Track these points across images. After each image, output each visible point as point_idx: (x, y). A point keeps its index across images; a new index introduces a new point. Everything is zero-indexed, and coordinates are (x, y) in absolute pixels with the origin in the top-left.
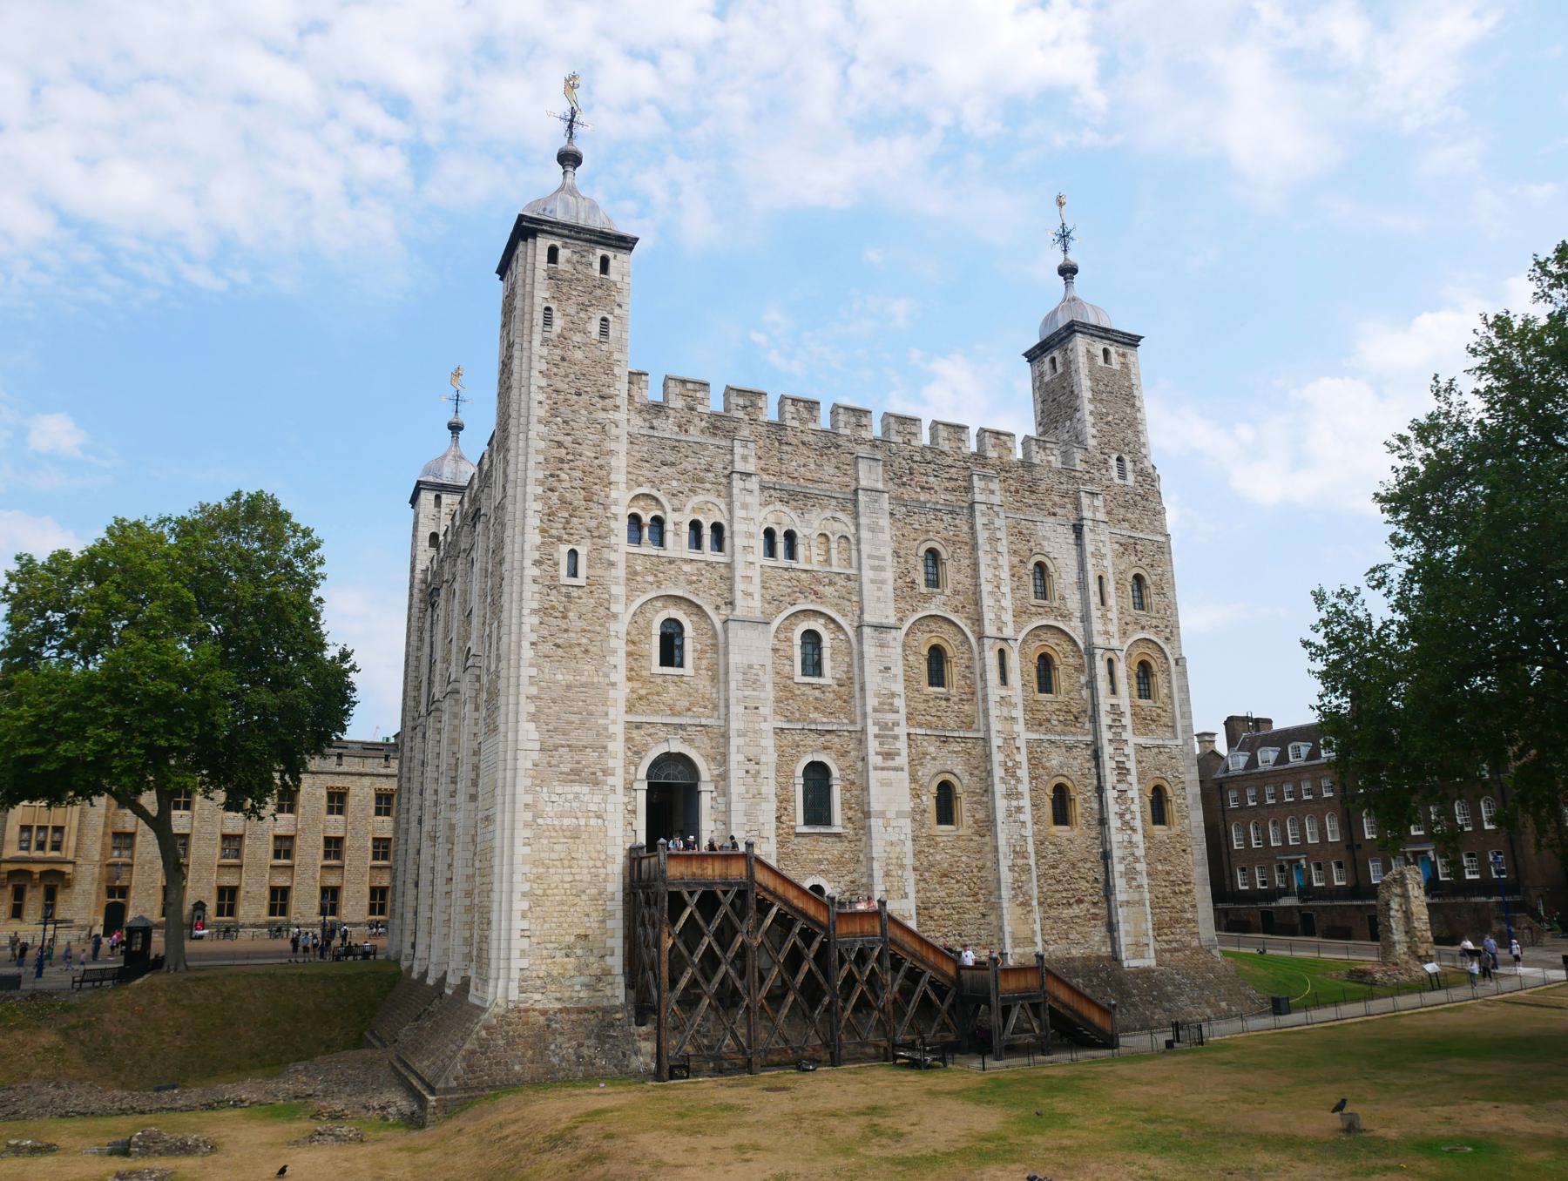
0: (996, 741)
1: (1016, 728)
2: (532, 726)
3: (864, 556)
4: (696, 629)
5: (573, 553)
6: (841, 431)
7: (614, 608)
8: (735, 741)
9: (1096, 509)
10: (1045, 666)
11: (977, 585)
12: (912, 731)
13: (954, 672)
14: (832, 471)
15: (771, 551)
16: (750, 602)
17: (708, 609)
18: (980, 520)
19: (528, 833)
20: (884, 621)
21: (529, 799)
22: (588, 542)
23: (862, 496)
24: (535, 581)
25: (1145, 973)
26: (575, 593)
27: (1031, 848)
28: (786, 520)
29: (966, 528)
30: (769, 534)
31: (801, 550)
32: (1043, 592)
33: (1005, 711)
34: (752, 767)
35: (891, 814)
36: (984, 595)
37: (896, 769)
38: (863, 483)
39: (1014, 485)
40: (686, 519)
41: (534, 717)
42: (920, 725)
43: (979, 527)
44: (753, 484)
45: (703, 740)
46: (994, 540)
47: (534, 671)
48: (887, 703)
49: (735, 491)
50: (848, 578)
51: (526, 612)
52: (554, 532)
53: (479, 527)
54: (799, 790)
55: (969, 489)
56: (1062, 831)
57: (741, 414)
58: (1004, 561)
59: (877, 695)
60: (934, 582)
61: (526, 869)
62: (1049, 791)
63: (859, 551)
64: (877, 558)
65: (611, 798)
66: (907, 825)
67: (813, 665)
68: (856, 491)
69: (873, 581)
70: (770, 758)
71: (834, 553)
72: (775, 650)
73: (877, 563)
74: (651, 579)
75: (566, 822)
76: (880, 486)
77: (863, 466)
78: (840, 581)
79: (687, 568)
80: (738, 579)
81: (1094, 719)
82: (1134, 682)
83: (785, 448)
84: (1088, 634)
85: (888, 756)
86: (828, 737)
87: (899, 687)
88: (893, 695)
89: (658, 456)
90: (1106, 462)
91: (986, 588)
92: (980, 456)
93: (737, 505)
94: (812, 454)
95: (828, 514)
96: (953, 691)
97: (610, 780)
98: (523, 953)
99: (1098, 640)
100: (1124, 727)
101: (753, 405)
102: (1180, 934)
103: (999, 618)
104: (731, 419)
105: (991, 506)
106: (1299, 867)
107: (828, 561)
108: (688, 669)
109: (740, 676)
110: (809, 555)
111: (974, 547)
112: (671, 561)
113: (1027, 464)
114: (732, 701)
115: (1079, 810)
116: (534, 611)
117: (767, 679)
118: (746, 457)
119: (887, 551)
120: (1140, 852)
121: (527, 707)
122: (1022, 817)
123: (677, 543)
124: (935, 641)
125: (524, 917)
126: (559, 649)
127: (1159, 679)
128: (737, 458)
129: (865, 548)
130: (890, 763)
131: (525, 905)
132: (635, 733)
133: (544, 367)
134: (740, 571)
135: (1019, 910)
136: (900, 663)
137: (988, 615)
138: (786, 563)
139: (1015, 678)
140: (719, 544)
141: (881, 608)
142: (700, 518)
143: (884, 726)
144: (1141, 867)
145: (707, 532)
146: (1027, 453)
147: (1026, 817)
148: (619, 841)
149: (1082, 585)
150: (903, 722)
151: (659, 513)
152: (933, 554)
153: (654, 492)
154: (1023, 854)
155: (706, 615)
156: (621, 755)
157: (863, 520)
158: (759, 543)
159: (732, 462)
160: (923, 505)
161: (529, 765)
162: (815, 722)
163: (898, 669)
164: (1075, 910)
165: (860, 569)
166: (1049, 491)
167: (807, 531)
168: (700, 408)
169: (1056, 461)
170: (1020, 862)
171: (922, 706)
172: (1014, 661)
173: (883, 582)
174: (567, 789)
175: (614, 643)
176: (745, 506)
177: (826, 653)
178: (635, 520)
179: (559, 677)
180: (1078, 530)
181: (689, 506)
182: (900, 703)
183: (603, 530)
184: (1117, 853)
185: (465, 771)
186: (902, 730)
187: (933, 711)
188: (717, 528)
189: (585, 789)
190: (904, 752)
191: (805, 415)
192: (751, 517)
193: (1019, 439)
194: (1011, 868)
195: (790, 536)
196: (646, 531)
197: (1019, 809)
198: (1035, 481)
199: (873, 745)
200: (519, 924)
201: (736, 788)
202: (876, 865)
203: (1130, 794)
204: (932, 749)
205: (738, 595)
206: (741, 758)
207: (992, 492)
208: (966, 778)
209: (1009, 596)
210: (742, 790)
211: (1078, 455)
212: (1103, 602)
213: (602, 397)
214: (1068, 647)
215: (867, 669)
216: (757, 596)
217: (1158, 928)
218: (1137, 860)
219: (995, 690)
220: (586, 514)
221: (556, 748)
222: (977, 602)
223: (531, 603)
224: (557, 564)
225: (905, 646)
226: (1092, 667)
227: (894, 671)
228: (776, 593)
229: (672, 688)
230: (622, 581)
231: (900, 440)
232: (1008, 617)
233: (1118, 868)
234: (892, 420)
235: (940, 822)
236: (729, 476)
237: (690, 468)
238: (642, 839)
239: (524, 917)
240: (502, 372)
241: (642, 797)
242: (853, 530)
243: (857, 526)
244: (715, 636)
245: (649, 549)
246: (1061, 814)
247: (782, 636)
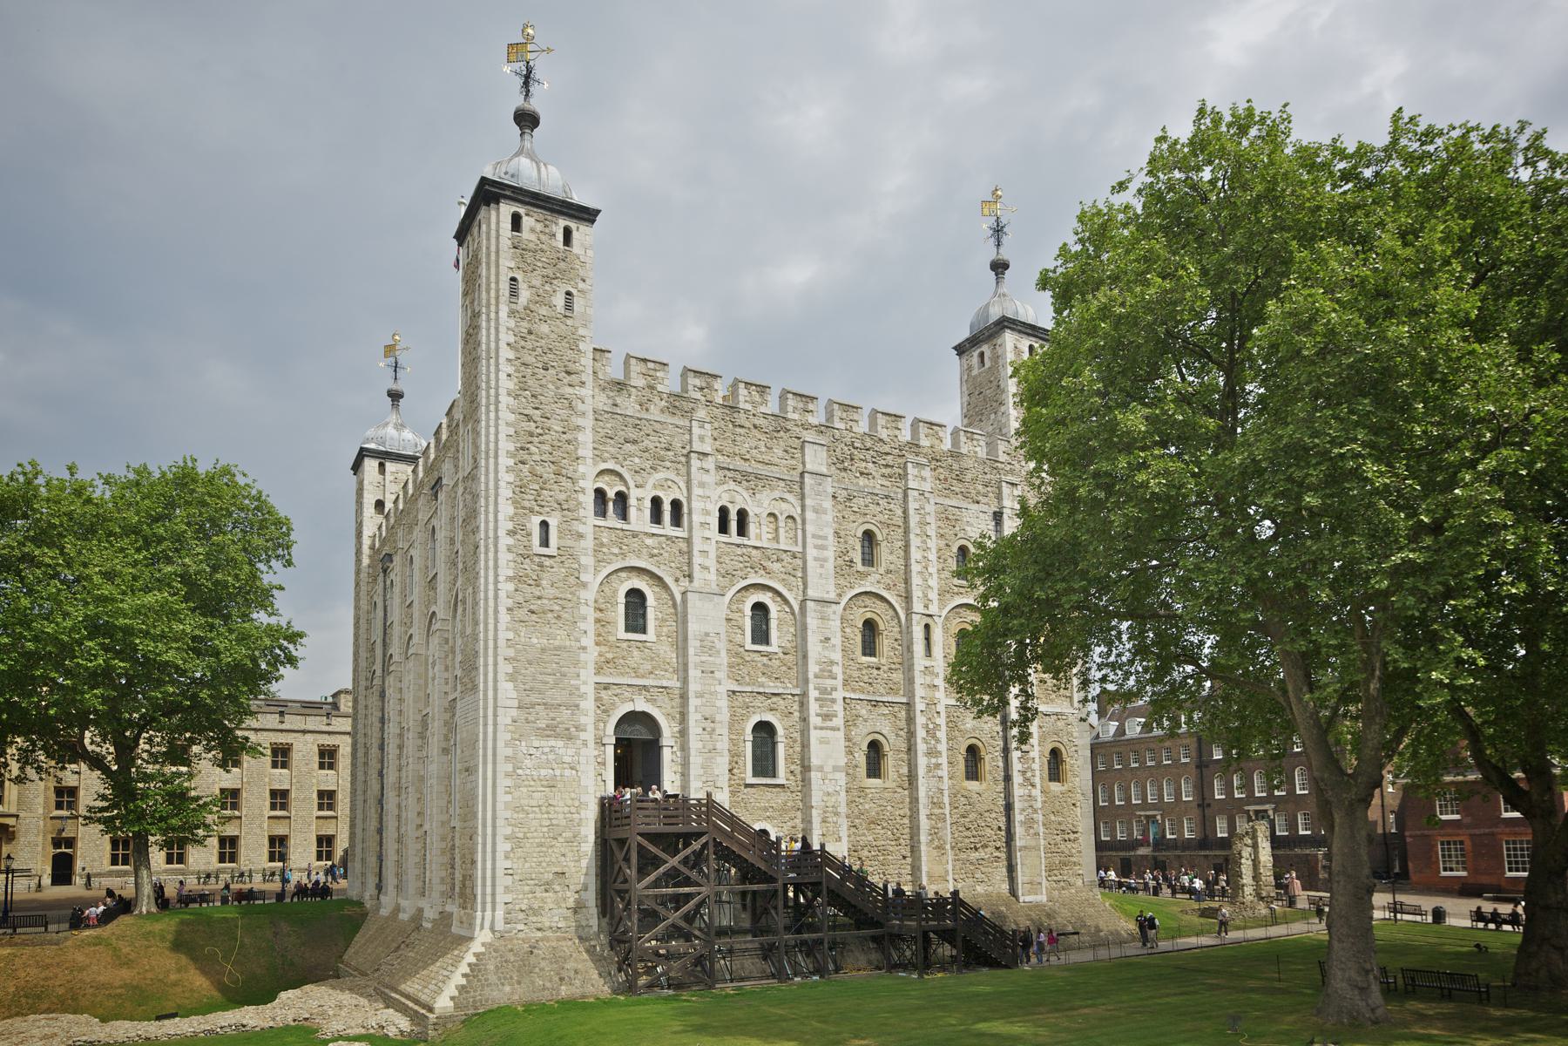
0: (920, 706)
1: (937, 695)
2: (510, 685)
3: (809, 536)
4: (657, 599)
5: (544, 525)
6: (790, 415)
7: (584, 578)
8: (693, 702)
11: (907, 566)
12: (848, 695)
13: (885, 643)
14: (780, 453)
15: (723, 528)
16: (706, 575)
17: (669, 580)
18: (912, 505)
19: (509, 782)
20: (826, 597)
21: (509, 752)
22: (557, 514)
24: (509, 550)
25: (1038, 906)
26: (548, 562)
27: (946, 800)
28: (738, 498)
29: (899, 512)
30: (724, 512)
31: (752, 528)
33: (928, 680)
34: (708, 725)
35: (828, 769)
36: (914, 574)
37: (833, 729)
38: (809, 467)
39: (943, 473)
40: (648, 494)
41: (512, 678)
42: (854, 691)
43: (911, 512)
44: (709, 463)
45: (663, 699)
46: (923, 524)
47: (511, 635)
48: (826, 671)
49: (693, 469)
51: (501, 579)
52: (526, 504)
53: (442, 496)
54: (749, 746)
55: (904, 476)
56: (973, 785)
57: (698, 395)
58: (933, 544)
59: (818, 663)
60: (869, 560)
61: (508, 814)
62: (963, 750)
63: (804, 531)
64: (820, 537)
65: (583, 751)
66: (842, 778)
67: (761, 635)
68: (802, 474)
69: (816, 559)
70: (724, 716)
71: (781, 531)
72: (728, 620)
73: (820, 542)
74: (616, 551)
75: (543, 772)
76: (824, 470)
77: (809, 449)
78: (787, 558)
79: (649, 541)
80: (695, 553)
83: (738, 430)
85: (827, 717)
86: (775, 699)
87: (837, 656)
88: (832, 663)
89: (621, 433)
91: (915, 568)
92: (914, 445)
93: (695, 482)
94: (763, 437)
95: (777, 494)
96: (883, 661)
97: (583, 735)
98: (507, 889)
101: (709, 387)
102: (1067, 874)
103: (926, 596)
104: (688, 399)
106: (1155, 822)
107: (776, 539)
108: (651, 635)
109: (698, 644)
110: (759, 532)
111: (907, 531)
113: (955, 455)
114: (691, 665)
115: (987, 768)
116: (509, 579)
117: (722, 646)
119: (829, 532)
120: (1039, 805)
121: (505, 668)
122: (940, 773)
123: (639, 516)
124: (869, 615)
125: (507, 858)
126: (530, 612)
128: (695, 438)
129: (810, 528)
130: (829, 724)
131: (508, 846)
132: (604, 694)
134: (698, 545)
135: (935, 853)
136: (839, 634)
137: (917, 593)
138: (739, 540)
139: (937, 650)
140: (677, 520)
141: (822, 583)
142: (661, 494)
143: (823, 691)
144: (1039, 817)
145: (667, 507)
146: (956, 443)
147: (944, 772)
148: (591, 790)
150: (840, 688)
151: (623, 489)
152: (869, 536)
153: (618, 468)
154: (939, 805)
155: (665, 586)
156: (591, 713)
157: (808, 502)
159: (691, 442)
161: (509, 721)
162: (762, 686)
163: (837, 640)
164: (981, 854)
165: (804, 546)
166: (974, 480)
168: (660, 388)
169: (982, 452)
170: (937, 811)
171: (856, 674)
172: (937, 635)
173: (825, 560)
174: (543, 743)
175: (584, 610)
176: (702, 485)
177: (773, 624)
178: (600, 494)
179: (535, 641)
181: (651, 481)
182: (837, 670)
183: (572, 504)
184: (1017, 806)
185: (436, 726)
186: (839, 695)
187: (866, 678)
188: (676, 505)
189: (560, 743)
190: (841, 714)
191: (757, 398)
193: (949, 430)
194: (929, 817)
195: (742, 515)
196: (611, 504)
197: (938, 766)
198: (963, 471)
199: (814, 707)
200: (502, 864)
201: (694, 744)
202: (814, 812)
203: (1032, 754)
204: (864, 712)
205: (696, 568)
206: (699, 716)
208: (892, 737)
209: (935, 576)
210: (700, 745)
211: (1002, 446)
215: (810, 639)
216: (713, 570)
217: (1050, 870)
218: (1035, 811)
219: (920, 661)
220: (555, 487)
221: (533, 706)
222: (907, 581)
223: (506, 571)
224: (529, 535)
227: (833, 641)
228: (730, 568)
229: (636, 653)
230: (590, 552)
231: (842, 426)
232: (933, 595)
233: (1018, 817)
234: (836, 407)
235: (869, 776)
236: (687, 456)
237: (651, 446)
238: (610, 790)
239: (507, 858)
240: (466, 342)
241: (610, 750)
243: (803, 507)
244: (674, 605)
245: (612, 520)
246: (973, 772)
247: (734, 607)
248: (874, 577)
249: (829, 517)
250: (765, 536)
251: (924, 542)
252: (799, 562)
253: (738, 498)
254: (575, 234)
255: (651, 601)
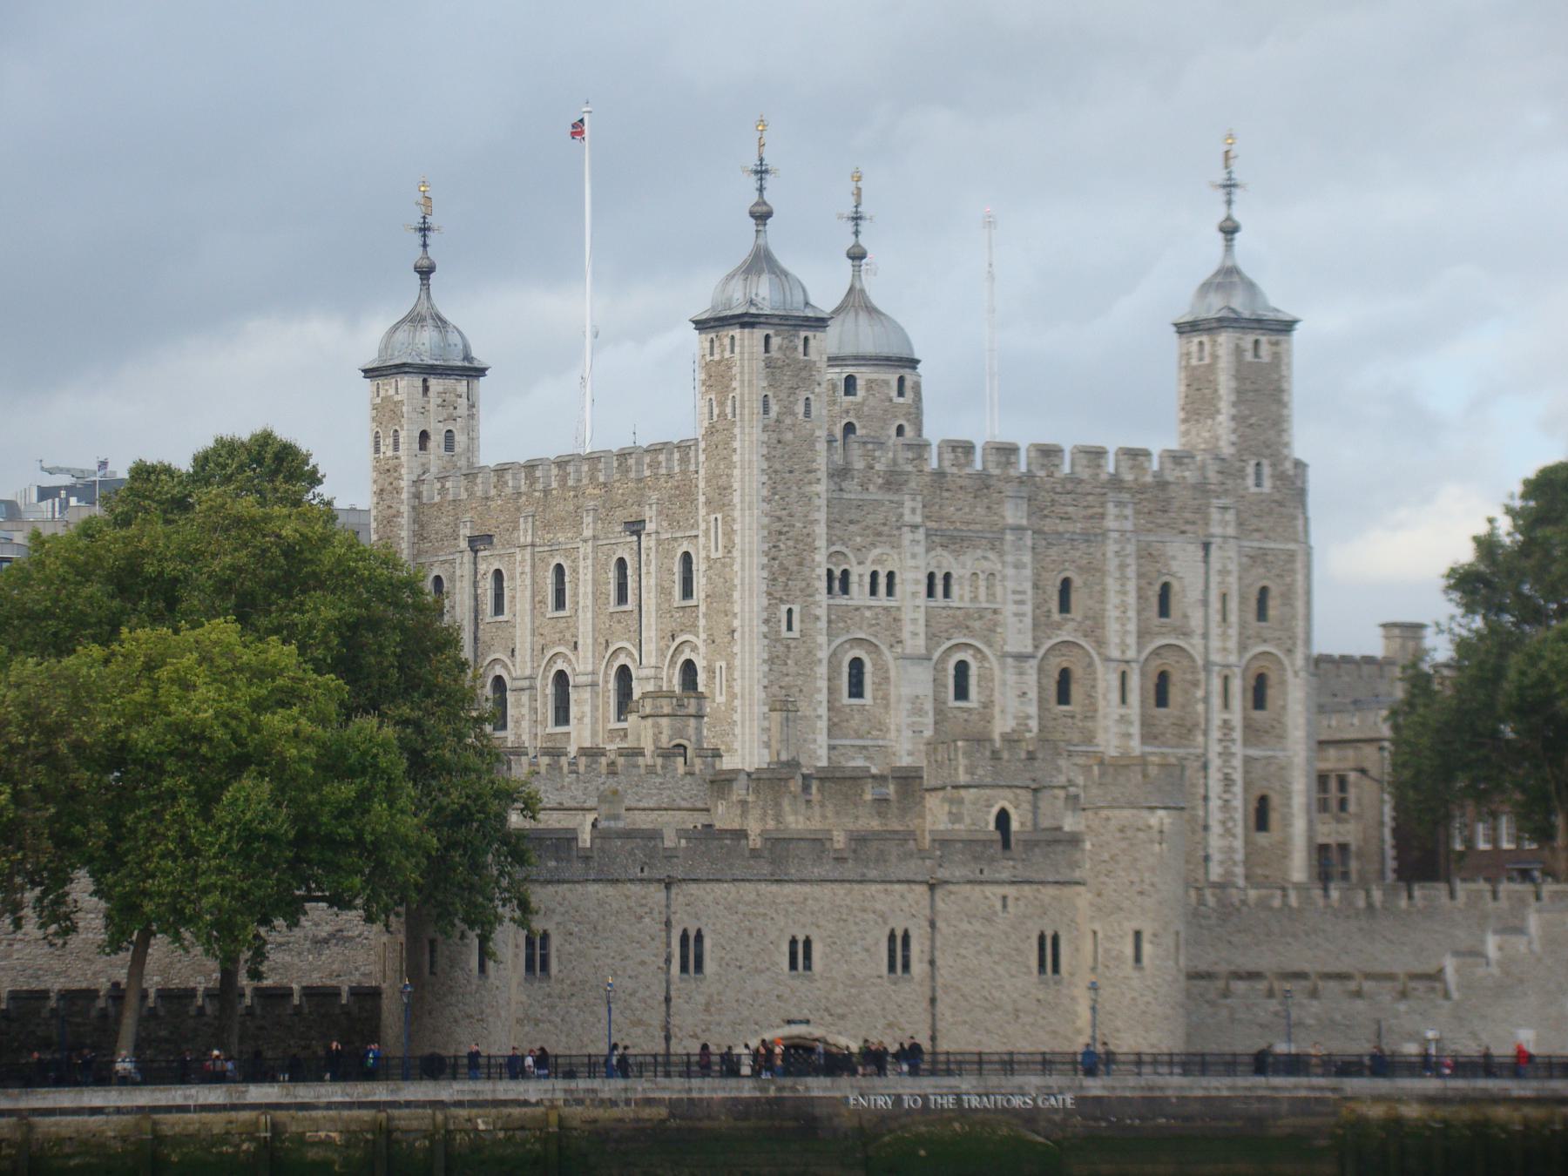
9: (1225, 524)
10: (1163, 681)
15: (930, 593)
17: (884, 648)
18: (1111, 548)
23: (1009, 537)
28: (945, 563)
29: (1099, 555)
30: (931, 576)
31: (955, 589)
32: (1164, 610)
38: (1010, 520)
40: (867, 571)
43: (1110, 555)
46: (1122, 567)
50: (995, 611)
60: (1065, 606)
63: (1005, 588)
67: (961, 692)
73: (1018, 597)
76: (1024, 522)
78: (989, 615)
79: (868, 614)
81: (1206, 733)
82: (1250, 695)
84: (1206, 648)
90: (1242, 470)
91: (1112, 613)
92: (1116, 482)
99: (1215, 657)
100: (1233, 741)
105: (1123, 532)
107: (974, 599)
112: (857, 609)
113: (1162, 485)
118: (911, 510)
119: (1028, 586)
123: (859, 591)
124: (1065, 665)
127: (1271, 693)
128: (907, 512)
129: (1010, 585)
133: (765, 451)
134: (906, 616)
136: (1035, 689)
139: (1134, 697)
141: (1017, 637)
142: (878, 568)
149: (1205, 603)
152: (1066, 585)
153: (844, 549)
157: (1009, 558)
158: (923, 589)
159: (901, 515)
160: (1060, 534)
165: (1004, 603)
166: (1182, 508)
167: (962, 572)
172: (1134, 681)
173: (1024, 615)
176: (914, 556)
180: (1206, 546)
188: (891, 575)
192: (911, 566)
195: (947, 577)
196: (836, 584)
198: (1168, 501)
205: (905, 635)
207: (1126, 518)
212: (1224, 619)
213: (809, 472)
214: (1185, 663)
225: (1040, 670)
226: (1207, 684)
232: (1132, 640)
236: (899, 528)
237: (871, 523)
242: (999, 566)
244: (887, 671)
248: (1070, 626)
249: (1028, 572)
250: (967, 598)
251: (1123, 585)
252: (1000, 617)
253: (946, 561)
254: (812, 343)
255: (868, 668)
